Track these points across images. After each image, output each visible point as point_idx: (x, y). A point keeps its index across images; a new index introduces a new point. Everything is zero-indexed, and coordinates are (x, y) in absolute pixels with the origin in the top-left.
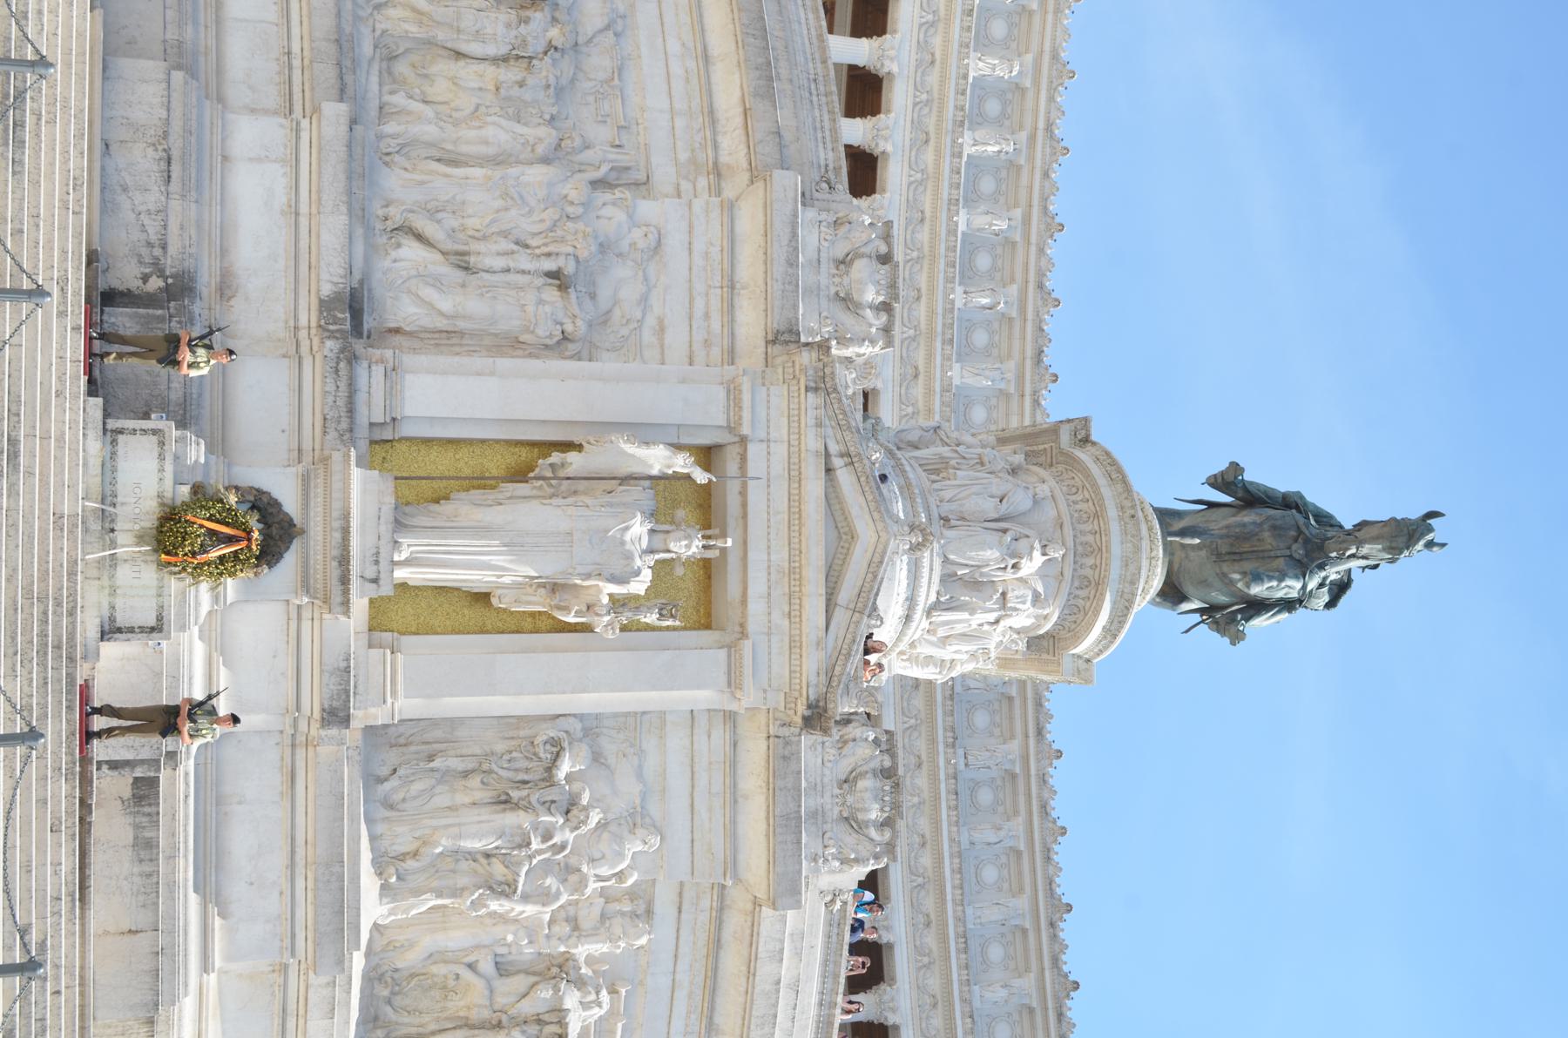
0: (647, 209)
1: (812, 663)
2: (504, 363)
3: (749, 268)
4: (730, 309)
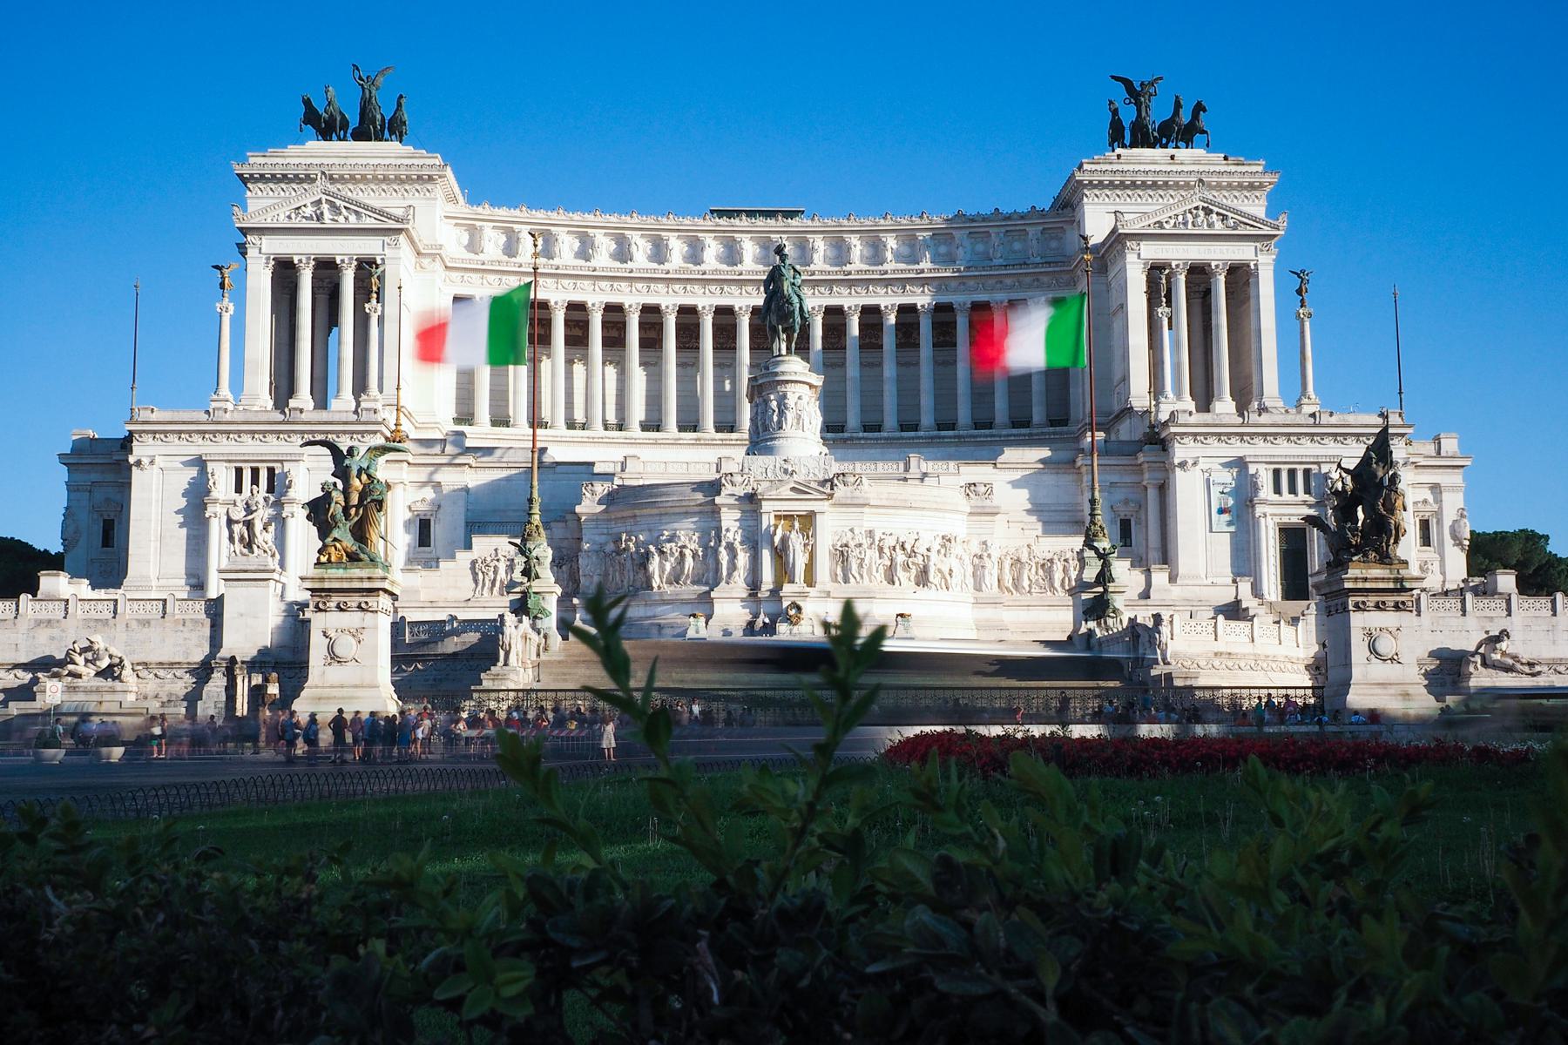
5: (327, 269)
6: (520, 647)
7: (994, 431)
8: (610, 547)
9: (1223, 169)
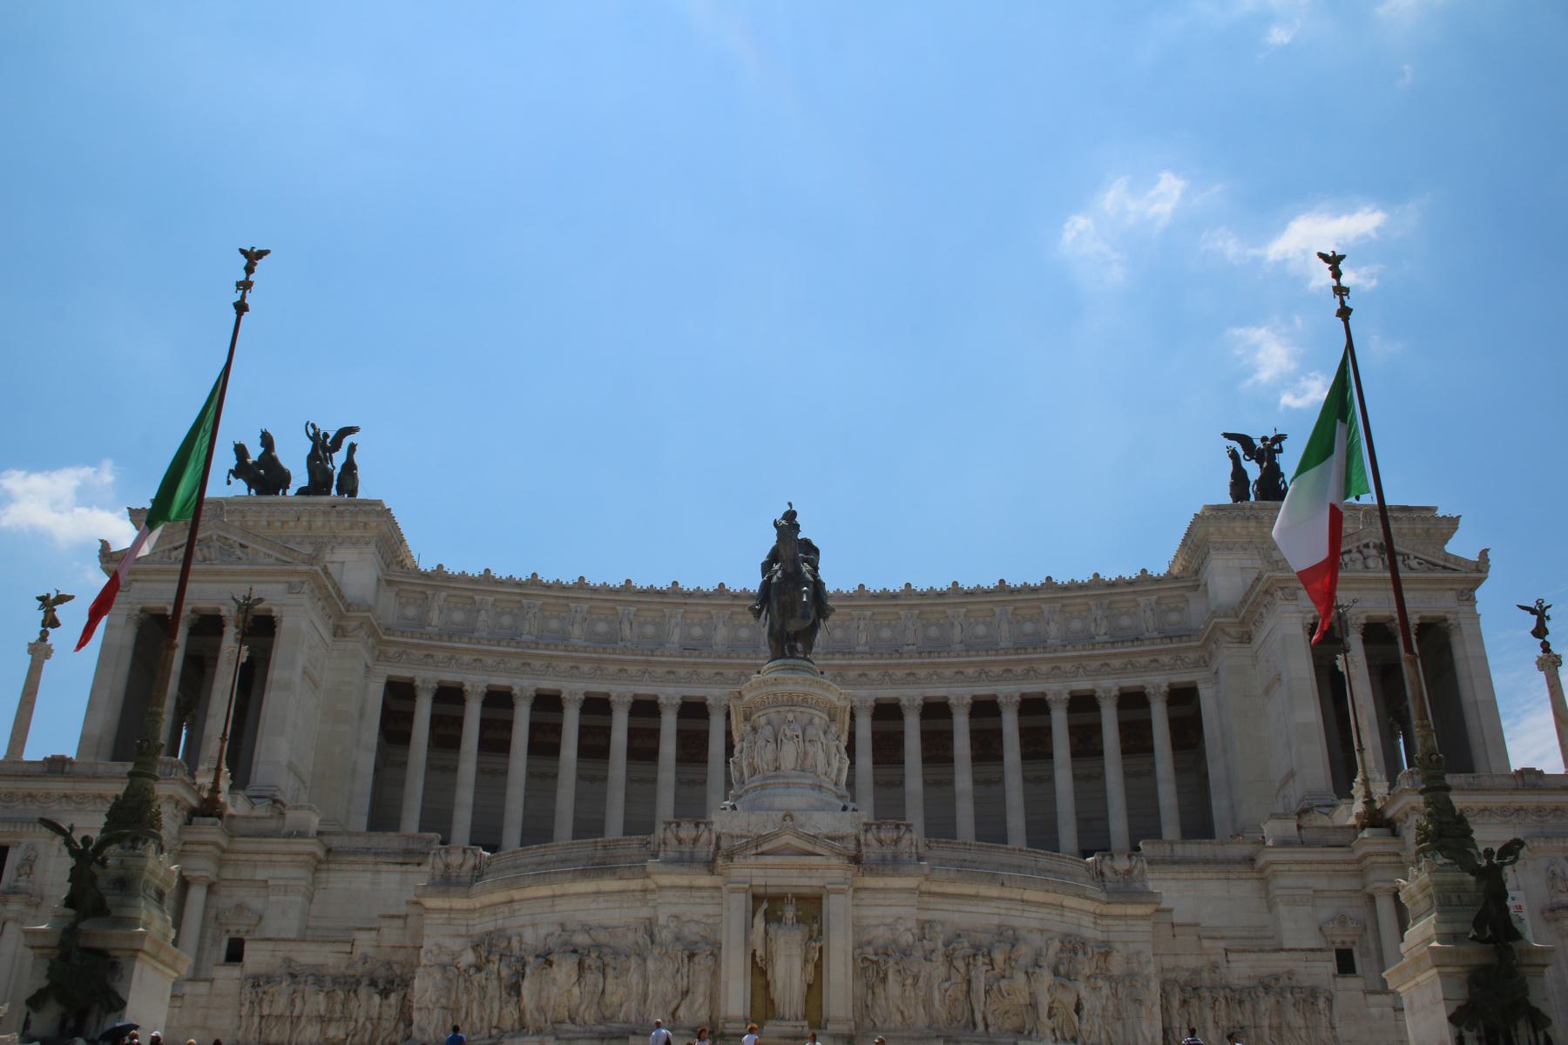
0: (662, 921)
1: (834, 861)
2: (723, 978)
3: (683, 880)
4: (700, 888)
5: (209, 625)
8: (468, 958)
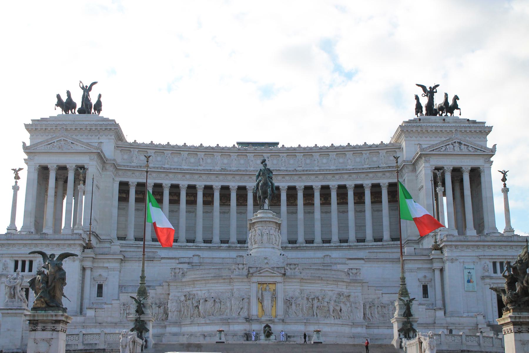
0: (235, 290)
6: (131, 346)
7: (366, 243)
8: (183, 298)
9: (467, 125)
